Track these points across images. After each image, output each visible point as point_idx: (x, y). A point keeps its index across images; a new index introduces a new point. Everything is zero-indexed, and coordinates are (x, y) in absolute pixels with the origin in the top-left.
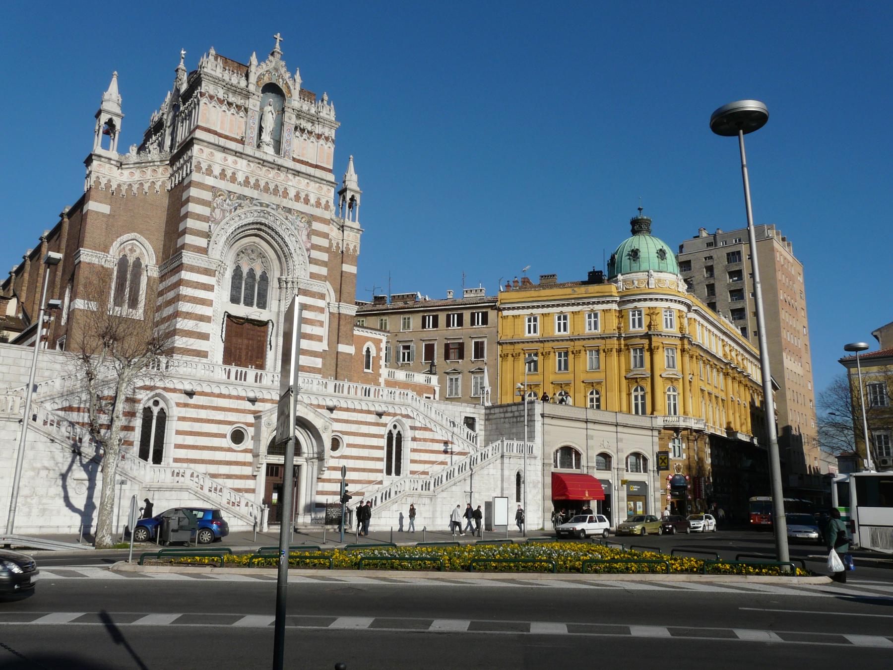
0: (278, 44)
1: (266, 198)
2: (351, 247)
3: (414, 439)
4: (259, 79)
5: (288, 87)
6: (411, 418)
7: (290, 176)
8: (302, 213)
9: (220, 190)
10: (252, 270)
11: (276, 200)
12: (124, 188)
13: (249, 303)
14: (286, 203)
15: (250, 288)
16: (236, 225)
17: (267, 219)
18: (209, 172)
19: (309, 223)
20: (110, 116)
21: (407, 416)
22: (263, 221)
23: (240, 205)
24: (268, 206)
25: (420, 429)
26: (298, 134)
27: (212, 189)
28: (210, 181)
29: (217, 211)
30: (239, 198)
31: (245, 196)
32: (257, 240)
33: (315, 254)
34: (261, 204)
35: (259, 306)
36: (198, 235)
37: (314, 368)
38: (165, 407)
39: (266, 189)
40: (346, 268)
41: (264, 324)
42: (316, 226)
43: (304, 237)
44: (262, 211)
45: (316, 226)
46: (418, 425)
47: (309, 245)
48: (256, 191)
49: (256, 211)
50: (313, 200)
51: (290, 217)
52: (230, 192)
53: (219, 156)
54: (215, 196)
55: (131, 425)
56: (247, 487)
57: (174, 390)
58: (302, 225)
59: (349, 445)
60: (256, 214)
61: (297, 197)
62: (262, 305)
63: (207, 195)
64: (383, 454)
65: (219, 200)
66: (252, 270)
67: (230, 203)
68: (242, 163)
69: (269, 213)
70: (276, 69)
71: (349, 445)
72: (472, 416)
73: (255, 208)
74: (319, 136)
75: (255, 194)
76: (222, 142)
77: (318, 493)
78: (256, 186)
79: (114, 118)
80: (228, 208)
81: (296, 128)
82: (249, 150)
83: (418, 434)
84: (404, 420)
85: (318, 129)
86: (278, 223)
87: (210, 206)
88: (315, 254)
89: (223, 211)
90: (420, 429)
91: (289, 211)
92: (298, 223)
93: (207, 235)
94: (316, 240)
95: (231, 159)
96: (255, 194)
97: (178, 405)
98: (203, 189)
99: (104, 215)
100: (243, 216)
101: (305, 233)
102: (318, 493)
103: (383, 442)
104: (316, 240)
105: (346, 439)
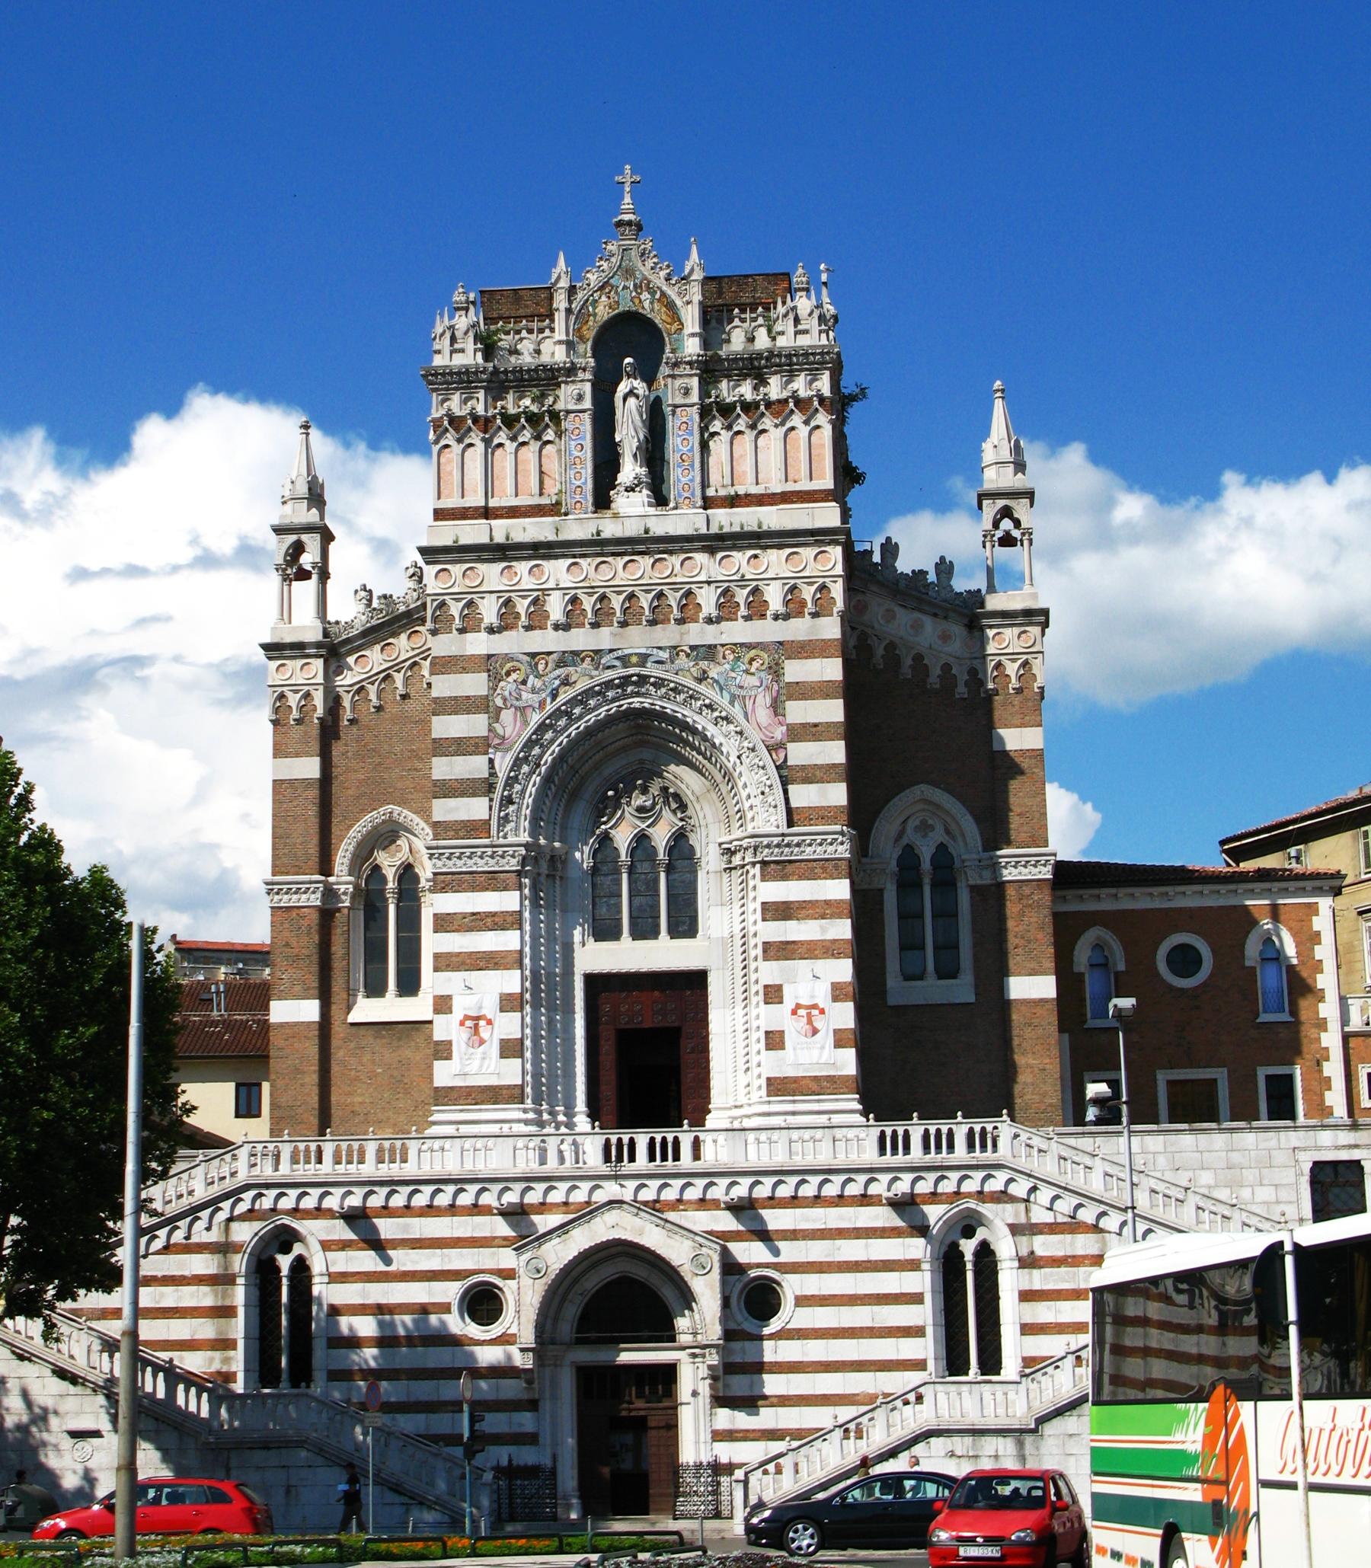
0: (627, 199)
1: (637, 639)
3: (1029, 1262)
5: (671, 306)
6: (1013, 1199)
7: (701, 558)
8: (750, 646)
10: (642, 839)
13: (645, 929)
14: (697, 634)
15: (645, 889)
16: (563, 739)
19: (776, 670)
20: (294, 538)
21: (1002, 1197)
22: (636, 702)
23: (566, 682)
24: (643, 659)
25: (1053, 1228)
27: (489, 663)
28: (478, 644)
29: (507, 716)
30: (561, 663)
31: (575, 653)
32: (646, 754)
34: (625, 661)
35: (674, 933)
36: (463, 794)
37: (830, 1079)
38: (305, 1253)
41: (695, 982)
42: (796, 670)
43: (763, 714)
44: (626, 680)
45: (796, 670)
46: (1040, 1216)
47: (779, 733)
49: (608, 685)
50: (775, 604)
52: (533, 655)
53: (491, 574)
54: (495, 679)
55: (228, 1303)
56: (515, 1429)
57: (319, 1212)
58: (753, 681)
59: (802, 1301)
60: (610, 694)
61: (726, 609)
62: (685, 925)
63: (474, 684)
64: (924, 1314)
65: (508, 686)
66: (642, 839)
67: (538, 683)
68: (557, 571)
69: (643, 680)
70: (629, 273)
71: (802, 1301)
72: (1344, 1155)
74: (778, 408)
75: (605, 638)
76: (501, 530)
77: (719, 1436)
79: (304, 537)
80: (535, 699)
82: (578, 527)
83: (1044, 1245)
84: (987, 1209)
85: (775, 388)
88: (800, 753)
89: (522, 710)
90: (1053, 1228)
91: (709, 652)
92: (742, 679)
93: (487, 787)
94: (799, 712)
95: (522, 567)
96: (605, 638)
97: (326, 1246)
98: (464, 670)
101: (764, 700)
102: (719, 1436)
103: (922, 1281)
104: (799, 712)
105: (791, 1286)
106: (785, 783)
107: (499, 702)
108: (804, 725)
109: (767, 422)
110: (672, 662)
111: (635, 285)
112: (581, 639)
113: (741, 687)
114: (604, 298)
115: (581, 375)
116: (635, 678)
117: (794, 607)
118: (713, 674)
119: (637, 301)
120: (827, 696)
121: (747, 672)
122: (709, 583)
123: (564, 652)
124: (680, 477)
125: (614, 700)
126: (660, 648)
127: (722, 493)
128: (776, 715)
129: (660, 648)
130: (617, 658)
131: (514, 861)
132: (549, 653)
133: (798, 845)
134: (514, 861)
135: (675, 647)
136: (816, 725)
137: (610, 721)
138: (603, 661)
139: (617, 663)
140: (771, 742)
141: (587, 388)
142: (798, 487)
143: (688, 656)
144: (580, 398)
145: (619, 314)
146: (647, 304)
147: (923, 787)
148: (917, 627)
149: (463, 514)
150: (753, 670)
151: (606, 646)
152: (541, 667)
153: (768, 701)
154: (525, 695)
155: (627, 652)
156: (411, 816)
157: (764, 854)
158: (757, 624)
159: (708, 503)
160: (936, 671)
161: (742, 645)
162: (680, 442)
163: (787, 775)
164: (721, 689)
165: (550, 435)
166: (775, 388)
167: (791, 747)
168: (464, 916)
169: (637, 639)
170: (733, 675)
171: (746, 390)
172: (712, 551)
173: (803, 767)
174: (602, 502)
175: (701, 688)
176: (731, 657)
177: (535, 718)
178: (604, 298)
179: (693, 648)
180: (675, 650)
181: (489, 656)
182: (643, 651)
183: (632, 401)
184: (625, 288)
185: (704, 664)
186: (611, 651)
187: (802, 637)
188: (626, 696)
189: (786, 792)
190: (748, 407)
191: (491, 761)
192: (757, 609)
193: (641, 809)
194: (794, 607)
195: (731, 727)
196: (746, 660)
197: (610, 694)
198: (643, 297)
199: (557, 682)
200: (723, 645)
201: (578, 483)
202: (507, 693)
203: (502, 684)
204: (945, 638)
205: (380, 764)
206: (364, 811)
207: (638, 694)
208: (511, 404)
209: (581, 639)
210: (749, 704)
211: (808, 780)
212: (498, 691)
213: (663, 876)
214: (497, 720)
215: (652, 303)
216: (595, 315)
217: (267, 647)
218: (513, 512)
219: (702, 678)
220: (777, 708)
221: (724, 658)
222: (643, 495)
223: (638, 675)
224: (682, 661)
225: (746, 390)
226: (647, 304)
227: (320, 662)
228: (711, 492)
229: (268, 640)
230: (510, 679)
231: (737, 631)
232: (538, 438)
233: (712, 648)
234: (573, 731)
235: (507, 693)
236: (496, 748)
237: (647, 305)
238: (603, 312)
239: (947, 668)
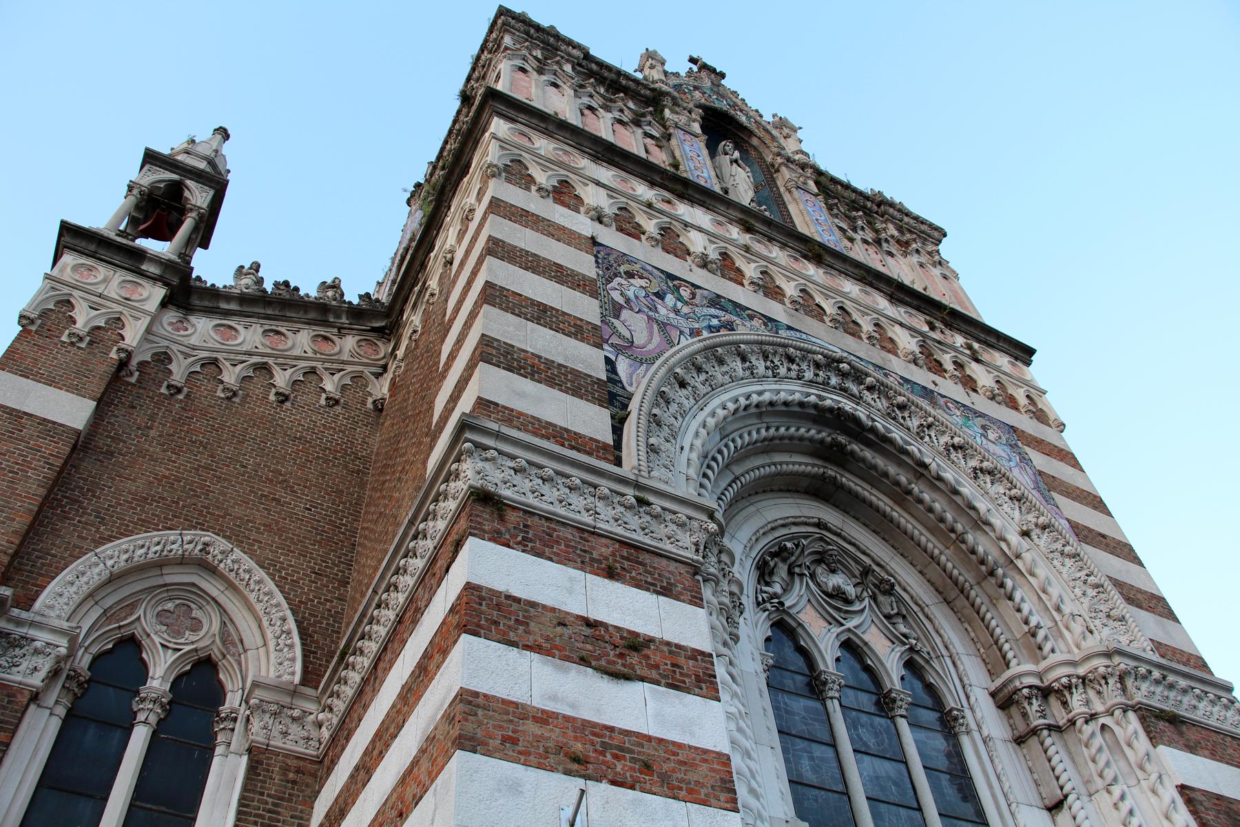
12: (178, 371)
17: (858, 399)
20: (175, 177)
22: (848, 406)
36: (551, 382)
87: (594, 294)
99: (49, 427)
116: (844, 366)
125: (811, 383)
131: (686, 539)
133: (1184, 691)
134: (686, 539)
136: (1103, 536)
154: (663, 311)
156: (247, 562)
157: (1142, 692)
168: (562, 619)
172: (892, 299)
186: (789, 328)
193: (838, 594)
197: (809, 375)
202: (630, 294)
205: (207, 468)
206: (146, 525)
213: (903, 724)
214: (617, 317)
227: (159, 292)
236: (619, 350)
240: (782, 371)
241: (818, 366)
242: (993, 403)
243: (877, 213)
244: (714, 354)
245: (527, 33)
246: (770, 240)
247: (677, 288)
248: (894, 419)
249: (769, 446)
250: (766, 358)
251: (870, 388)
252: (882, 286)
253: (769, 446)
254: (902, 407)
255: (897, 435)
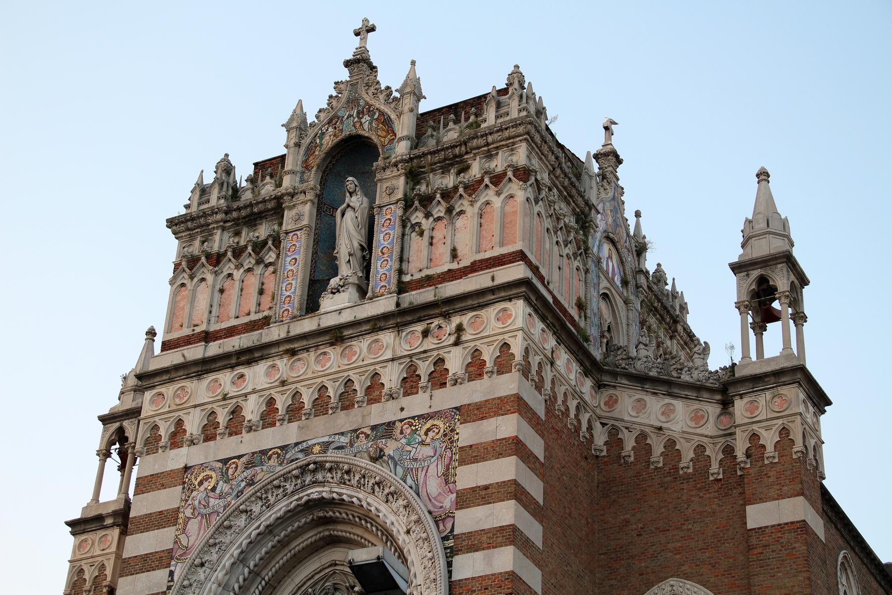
2: (769, 439)
4: (310, 151)
7: (387, 337)
9: (203, 466)
11: (345, 421)
14: (379, 413)
16: (243, 540)
17: (322, 483)
18: (177, 438)
19: (449, 436)
20: (117, 425)
22: (314, 493)
23: (251, 483)
24: (325, 446)
26: (418, 217)
29: (193, 525)
30: (250, 465)
31: (264, 452)
33: (469, 520)
34: (307, 451)
39: (321, 406)
40: (759, 515)
43: (434, 485)
44: (304, 469)
47: (448, 501)
48: (294, 425)
49: (285, 477)
51: (390, 448)
52: (225, 461)
53: (201, 390)
54: (189, 489)
58: (427, 451)
61: (410, 384)
65: (199, 495)
68: (257, 375)
69: (319, 466)
73: (293, 465)
78: (294, 411)
80: (222, 503)
81: (408, 204)
86: (354, 482)
89: (207, 517)
91: (386, 430)
94: (469, 476)
98: (163, 486)
100: (256, 508)
101: (436, 469)
104: (469, 476)
106: (451, 553)
107: (188, 512)
108: (473, 489)
109: (463, 204)
110: (352, 445)
111: (358, 113)
112: (270, 438)
113: (416, 460)
114: (330, 129)
115: (302, 197)
116: (312, 466)
117: (475, 369)
118: (389, 451)
119: (358, 125)
120: (499, 455)
121: (422, 443)
122: (393, 360)
123: (253, 453)
124: (383, 269)
126: (342, 434)
127: (417, 276)
128: (447, 482)
129: (342, 434)
130: (302, 451)
132: (239, 457)
135: (355, 431)
136: (486, 488)
137: (291, 514)
138: (288, 456)
139: (300, 455)
140: (437, 512)
141: (307, 208)
142: (488, 255)
143: (367, 436)
144: (299, 217)
145: (342, 141)
146: (366, 126)
147: (672, 581)
148: (668, 411)
149: (188, 341)
150: (428, 440)
151: (293, 441)
152: (230, 471)
153: (441, 470)
154: (212, 501)
155: (310, 443)
158: (439, 393)
159: (402, 288)
160: (688, 454)
161: (420, 417)
162: (386, 238)
163: (455, 545)
164: (396, 465)
165: (271, 257)
166: (476, 170)
167: (459, 514)
169: (319, 430)
170: (409, 448)
171: (450, 181)
172: (399, 327)
173: (470, 535)
174: (311, 306)
175: (376, 467)
176: (409, 431)
177: (215, 520)
178: (330, 129)
179: (374, 428)
180: (356, 432)
181: (186, 468)
182: (326, 439)
183: (349, 214)
184: (350, 116)
185: (381, 443)
186: (297, 444)
187: (477, 398)
188: (304, 487)
189: (450, 564)
190: (447, 195)
191: (171, 574)
192: (439, 378)
194: (475, 369)
195: (401, 502)
196: (422, 432)
197: (290, 487)
198: (363, 120)
199: (243, 484)
200: (401, 421)
201: (288, 294)
203: (195, 493)
204: (698, 418)
207: (315, 483)
208: (246, 236)
209: (270, 438)
210: (421, 476)
211: (474, 548)
212: (190, 502)
215: (370, 123)
216: (322, 145)
217: (69, 524)
218: (231, 332)
219: (378, 457)
220: (447, 477)
221: (402, 433)
222: (348, 296)
223: (315, 463)
224: (362, 443)
225: (450, 181)
226: (366, 126)
228: (407, 278)
229: (77, 515)
230: (202, 488)
231: (418, 404)
232: (259, 262)
233: (390, 425)
234: (253, 531)
235: (196, 503)
237: (367, 127)
238: (329, 141)
239: (700, 449)
240: (272, 500)
241: (297, 477)
242: (458, 386)
243: (467, 153)
244: (223, 528)
245: (188, 229)
246: (307, 350)
247: (227, 469)
248: (345, 483)
249: (283, 544)
250: (261, 498)
251: (330, 470)
252: (391, 322)
253: (283, 544)
254: (348, 472)
255: (346, 493)
